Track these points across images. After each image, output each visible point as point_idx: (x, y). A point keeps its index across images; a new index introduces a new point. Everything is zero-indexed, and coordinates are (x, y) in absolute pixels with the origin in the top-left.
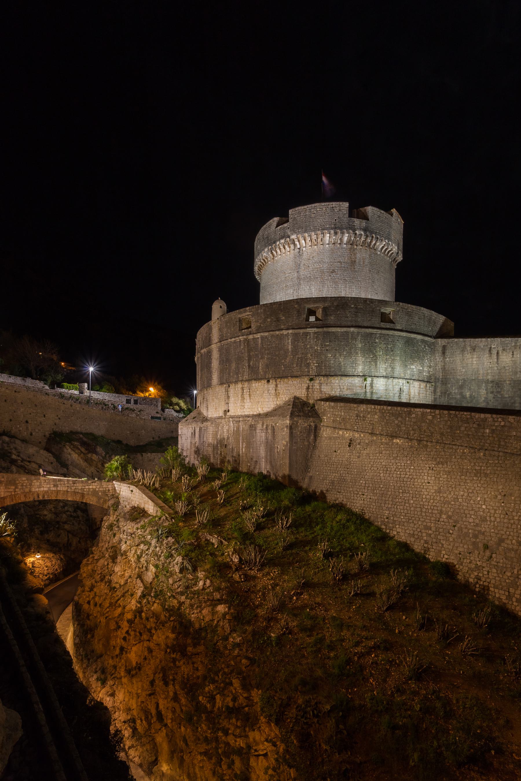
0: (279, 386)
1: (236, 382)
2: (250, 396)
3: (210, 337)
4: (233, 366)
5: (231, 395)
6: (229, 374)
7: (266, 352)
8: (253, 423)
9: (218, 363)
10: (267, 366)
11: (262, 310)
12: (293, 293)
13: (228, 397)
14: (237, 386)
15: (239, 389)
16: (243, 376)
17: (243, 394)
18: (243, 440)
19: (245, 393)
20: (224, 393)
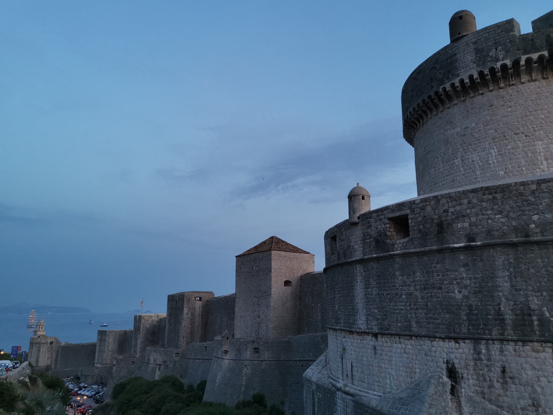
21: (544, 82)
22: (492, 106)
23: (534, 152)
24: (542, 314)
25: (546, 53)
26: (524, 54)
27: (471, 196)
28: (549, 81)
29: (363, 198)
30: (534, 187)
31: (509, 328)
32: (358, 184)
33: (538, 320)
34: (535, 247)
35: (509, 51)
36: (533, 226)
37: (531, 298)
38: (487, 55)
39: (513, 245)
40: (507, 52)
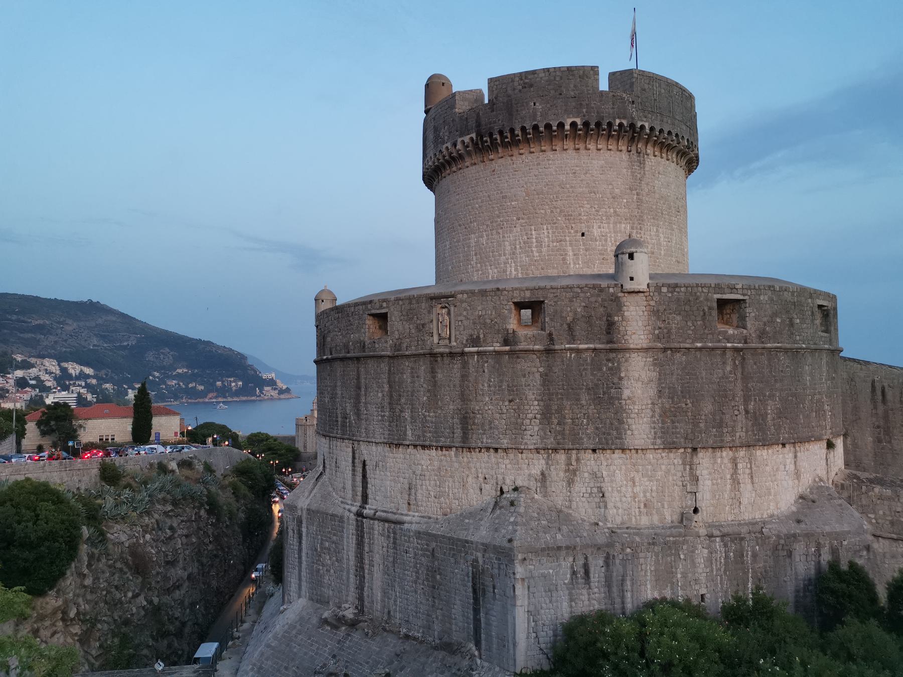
0: (799, 454)
4: (708, 407)
5: (705, 472)
6: (696, 424)
7: (778, 385)
9: (652, 392)
10: (780, 414)
11: (766, 298)
13: (695, 479)
15: (726, 461)
16: (734, 431)
19: (740, 472)
20: (681, 468)
21: (482, 165)
23: (469, 247)
24: (350, 418)
25: (474, 135)
26: (460, 137)
28: (486, 165)
29: (323, 301)
31: (339, 428)
32: (325, 286)
33: (349, 421)
34: (350, 362)
37: (347, 405)
39: (342, 359)
40: (450, 133)
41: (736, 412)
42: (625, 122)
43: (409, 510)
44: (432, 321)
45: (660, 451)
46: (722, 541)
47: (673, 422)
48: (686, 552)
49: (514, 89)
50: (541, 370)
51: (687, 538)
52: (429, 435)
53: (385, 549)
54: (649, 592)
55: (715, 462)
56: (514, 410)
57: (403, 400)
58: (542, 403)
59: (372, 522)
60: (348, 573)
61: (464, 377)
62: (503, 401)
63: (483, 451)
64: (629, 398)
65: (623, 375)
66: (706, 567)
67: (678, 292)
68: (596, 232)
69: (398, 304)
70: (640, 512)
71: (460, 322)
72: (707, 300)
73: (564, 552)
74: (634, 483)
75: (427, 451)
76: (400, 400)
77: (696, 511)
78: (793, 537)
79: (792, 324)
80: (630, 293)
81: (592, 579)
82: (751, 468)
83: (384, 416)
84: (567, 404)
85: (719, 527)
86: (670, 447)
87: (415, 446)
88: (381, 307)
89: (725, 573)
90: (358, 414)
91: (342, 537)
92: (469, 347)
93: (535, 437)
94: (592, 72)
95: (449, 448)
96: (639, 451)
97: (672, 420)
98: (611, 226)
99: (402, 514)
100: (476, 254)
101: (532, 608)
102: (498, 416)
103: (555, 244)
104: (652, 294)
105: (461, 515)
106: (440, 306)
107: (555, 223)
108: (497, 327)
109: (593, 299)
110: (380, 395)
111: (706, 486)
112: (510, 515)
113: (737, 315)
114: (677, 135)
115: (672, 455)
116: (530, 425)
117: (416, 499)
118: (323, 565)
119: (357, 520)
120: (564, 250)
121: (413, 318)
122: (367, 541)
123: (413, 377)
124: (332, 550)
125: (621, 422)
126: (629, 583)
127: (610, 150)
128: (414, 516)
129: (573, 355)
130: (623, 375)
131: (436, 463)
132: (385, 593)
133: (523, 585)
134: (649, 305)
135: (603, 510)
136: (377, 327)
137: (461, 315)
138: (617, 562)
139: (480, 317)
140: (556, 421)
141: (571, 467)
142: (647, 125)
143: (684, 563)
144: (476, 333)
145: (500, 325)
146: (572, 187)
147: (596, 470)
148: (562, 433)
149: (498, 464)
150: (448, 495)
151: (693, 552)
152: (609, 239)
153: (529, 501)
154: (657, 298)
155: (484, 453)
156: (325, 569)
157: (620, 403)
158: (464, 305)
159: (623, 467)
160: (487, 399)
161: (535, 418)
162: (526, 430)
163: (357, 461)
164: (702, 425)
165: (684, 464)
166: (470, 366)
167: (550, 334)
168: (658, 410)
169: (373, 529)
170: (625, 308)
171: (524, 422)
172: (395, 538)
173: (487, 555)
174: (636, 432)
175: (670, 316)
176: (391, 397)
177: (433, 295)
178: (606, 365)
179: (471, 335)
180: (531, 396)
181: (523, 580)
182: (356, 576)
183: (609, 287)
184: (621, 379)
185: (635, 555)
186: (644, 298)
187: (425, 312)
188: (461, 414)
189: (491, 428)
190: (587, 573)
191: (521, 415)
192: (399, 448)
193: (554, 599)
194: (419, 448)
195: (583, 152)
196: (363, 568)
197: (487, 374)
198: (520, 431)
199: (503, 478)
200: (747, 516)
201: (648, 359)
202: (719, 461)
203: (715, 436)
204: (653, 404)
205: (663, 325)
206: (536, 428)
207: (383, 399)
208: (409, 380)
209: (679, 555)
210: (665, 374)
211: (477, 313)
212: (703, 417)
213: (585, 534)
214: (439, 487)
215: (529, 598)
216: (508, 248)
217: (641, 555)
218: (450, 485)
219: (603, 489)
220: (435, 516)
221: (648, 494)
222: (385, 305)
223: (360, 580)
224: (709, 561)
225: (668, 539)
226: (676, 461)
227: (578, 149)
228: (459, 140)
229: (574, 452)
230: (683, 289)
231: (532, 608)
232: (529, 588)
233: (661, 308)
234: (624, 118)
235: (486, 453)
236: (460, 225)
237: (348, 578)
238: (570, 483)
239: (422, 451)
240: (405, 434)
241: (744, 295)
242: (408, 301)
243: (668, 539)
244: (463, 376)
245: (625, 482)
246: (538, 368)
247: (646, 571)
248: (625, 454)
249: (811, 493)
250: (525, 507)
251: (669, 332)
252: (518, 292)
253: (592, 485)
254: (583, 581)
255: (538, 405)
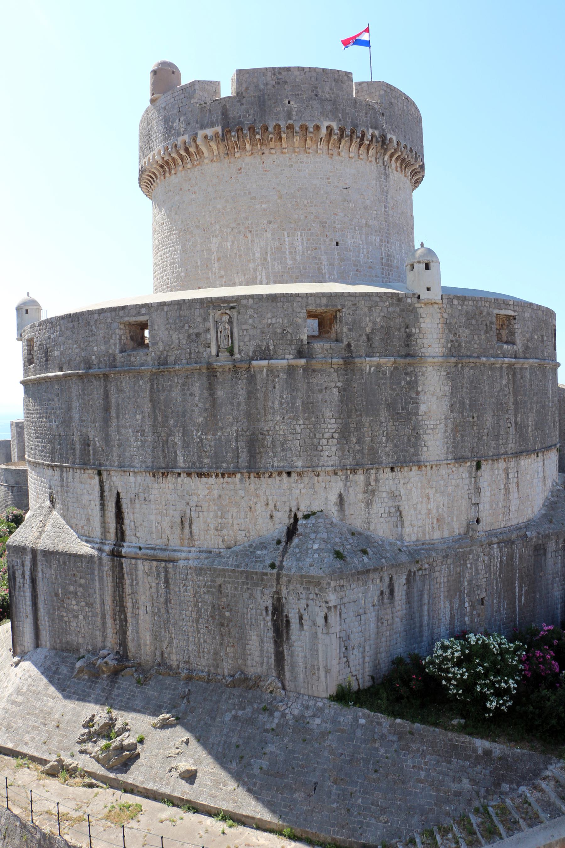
1: (496, 457)
2: (518, 487)
3: (409, 336)
4: (489, 420)
5: (486, 484)
6: (480, 439)
8: (540, 542)
9: (445, 406)
12: (380, 245)
13: (478, 490)
14: (496, 466)
15: (501, 472)
16: (507, 443)
17: (506, 484)
18: (521, 577)
19: (510, 481)
20: (467, 481)
22: (181, 189)
27: (62, 322)
30: (96, 317)
32: (28, 294)
33: (94, 449)
35: (189, 124)
36: (93, 357)
37: (89, 429)
38: (172, 127)
41: (509, 425)
42: (377, 133)
43: (182, 545)
44: (208, 330)
45: (451, 466)
46: (498, 547)
47: (462, 436)
48: (472, 561)
49: (267, 84)
50: (339, 384)
51: (473, 548)
52: (206, 461)
53: (153, 590)
54: (442, 603)
55: (494, 474)
56: (310, 429)
57: (171, 422)
58: (340, 421)
59: (133, 561)
60: (104, 616)
61: (251, 394)
62: (298, 420)
63: (273, 475)
64: (425, 413)
65: (420, 389)
66: (486, 573)
67: (467, 306)
68: (350, 242)
69: (163, 310)
70: (433, 528)
71: (245, 332)
72: (488, 314)
73: (371, 576)
74: (429, 499)
75: (204, 479)
76: (167, 422)
77: (478, 521)
78: (547, 536)
79: (543, 342)
80: (425, 304)
81: (396, 598)
82: (517, 477)
83: (145, 441)
84: (366, 420)
85: (495, 535)
86: (460, 459)
87: (189, 474)
88: (139, 314)
89: (500, 576)
90: (107, 439)
91: (93, 580)
92: (257, 360)
93: (333, 458)
94: (346, 78)
95: (232, 474)
96: (434, 467)
97: (461, 434)
98: (364, 237)
99: (175, 551)
100: (219, 259)
101: (343, 634)
102: (290, 437)
103: (309, 252)
104: (445, 306)
105: (251, 546)
106: (219, 312)
107: (310, 230)
108: (289, 337)
109: (391, 309)
110: (139, 417)
111: (486, 495)
112: (312, 542)
113: (507, 331)
114: (416, 154)
115: (461, 469)
116: (327, 445)
117: (191, 533)
118: (68, 610)
119: (113, 560)
120: (320, 259)
121: (183, 327)
122: (128, 582)
123: (184, 395)
124: (79, 594)
125: (418, 437)
126: (426, 597)
127: (361, 159)
128: (190, 552)
129: (372, 369)
130: (420, 389)
131: (216, 493)
132: (156, 637)
133: (335, 611)
134: (443, 317)
135: (400, 529)
136: (129, 338)
137: (246, 323)
138: (417, 578)
139: (269, 325)
140: (355, 440)
141: (370, 488)
142: (394, 138)
143: (470, 571)
144: (265, 343)
145: (293, 335)
146: (326, 193)
147: (393, 489)
148: (361, 451)
149: (290, 489)
150: (233, 525)
151: (477, 560)
152: (362, 251)
153: (329, 526)
154: (449, 310)
155: (275, 477)
156: (71, 615)
157: (417, 419)
158: (250, 311)
159: (420, 485)
160: (278, 418)
161: (333, 437)
162: (322, 450)
163: (106, 494)
164: (484, 438)
165: (470, 477)
166: (258, 381)
167: (349, 345)
168: (450, 425)
169: (136, 569)
170: (421, 320)
171: (321, 442)
172: (166, 576)
173: (291, 587)
174: (431, 449)
175: (461, 330)
176: (155, 418)
177: (209, 300)
178: (405, 379)
179: (259, 346)
180: (328, 414)
181: (335, 607)
182: (115, 620)
183: (407, 297)
184: (418, 393)
185: (432, 570)
186: (438, 310)
187: (199, 319)
188: (247, 436)
189: (283, 450)
190: (392, 592)
191: (317, 434)
192: (166, 477)
193: (363, 622)
194: (194, 476)
195: (336, 157)
196: (124, 611)
197: (277, 392)
198: (316, 452)
199: (298, 504)
200: (514, 522)
201: (442, 373)
202: (496, 472)
203: (494, 448)
204: (446, 418)
205: (454, 339)
206: (334, 449)
207: (143, 421)
208: (179, 399)
209: (466, 564)
210: (456, 388)
211: (266, 321)
212: (486, 431)
213: (388, 555)
214: (221, 518)
215: (341, 625)
216: (258, 255)
217: (437, 569)
218: (234, 514)
219: (401, 508)
220: (217, 550)
221: (440, 510)
222: (143, 311)
223: (121, 626)
224: (488, 567)
225: (458, 550)
226: (464, 475)
227: (332, 154)
228: (201, 133)
229: (373, 471)
230: (470, 303)
231: (343, 634)
232: (340, 614)
233: (453, 322)
234: (376, 128)
235: (278, 478)
236: (197, 227)
237: (104, 623)
238: (369, 504)
239: (196, 479)
240: (175, 460)
241: (514, 311)
242: (176, 307)
243: (458, 550)
244: (249, 392)
245: (420, 499)
246: (335, 382)
247: (440, 583)
248: (421, 471)
249: (553, 496)
250: (327, 533)
251: (459, 345)
252: (313, 298)
253: (390, 504)
254: (388, 601)
255: (336, 423)
